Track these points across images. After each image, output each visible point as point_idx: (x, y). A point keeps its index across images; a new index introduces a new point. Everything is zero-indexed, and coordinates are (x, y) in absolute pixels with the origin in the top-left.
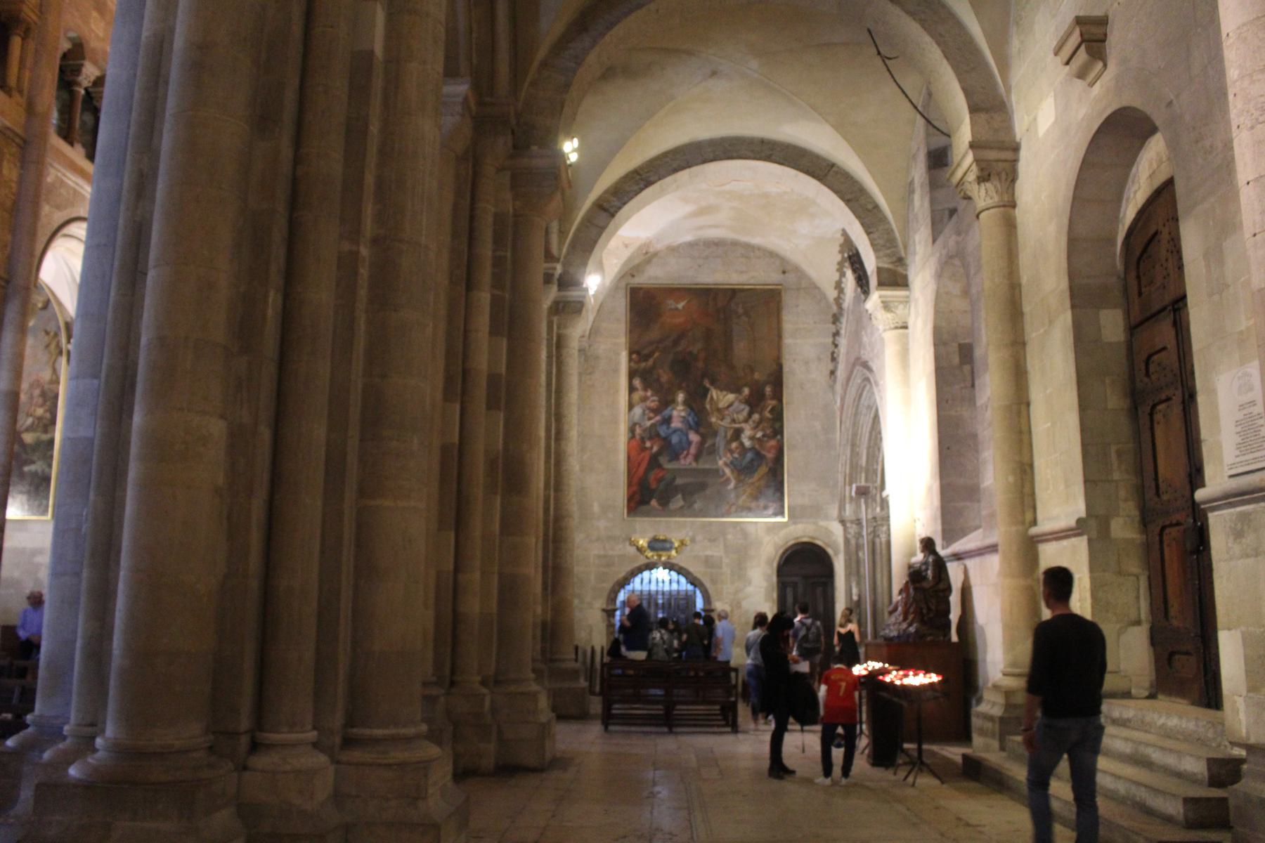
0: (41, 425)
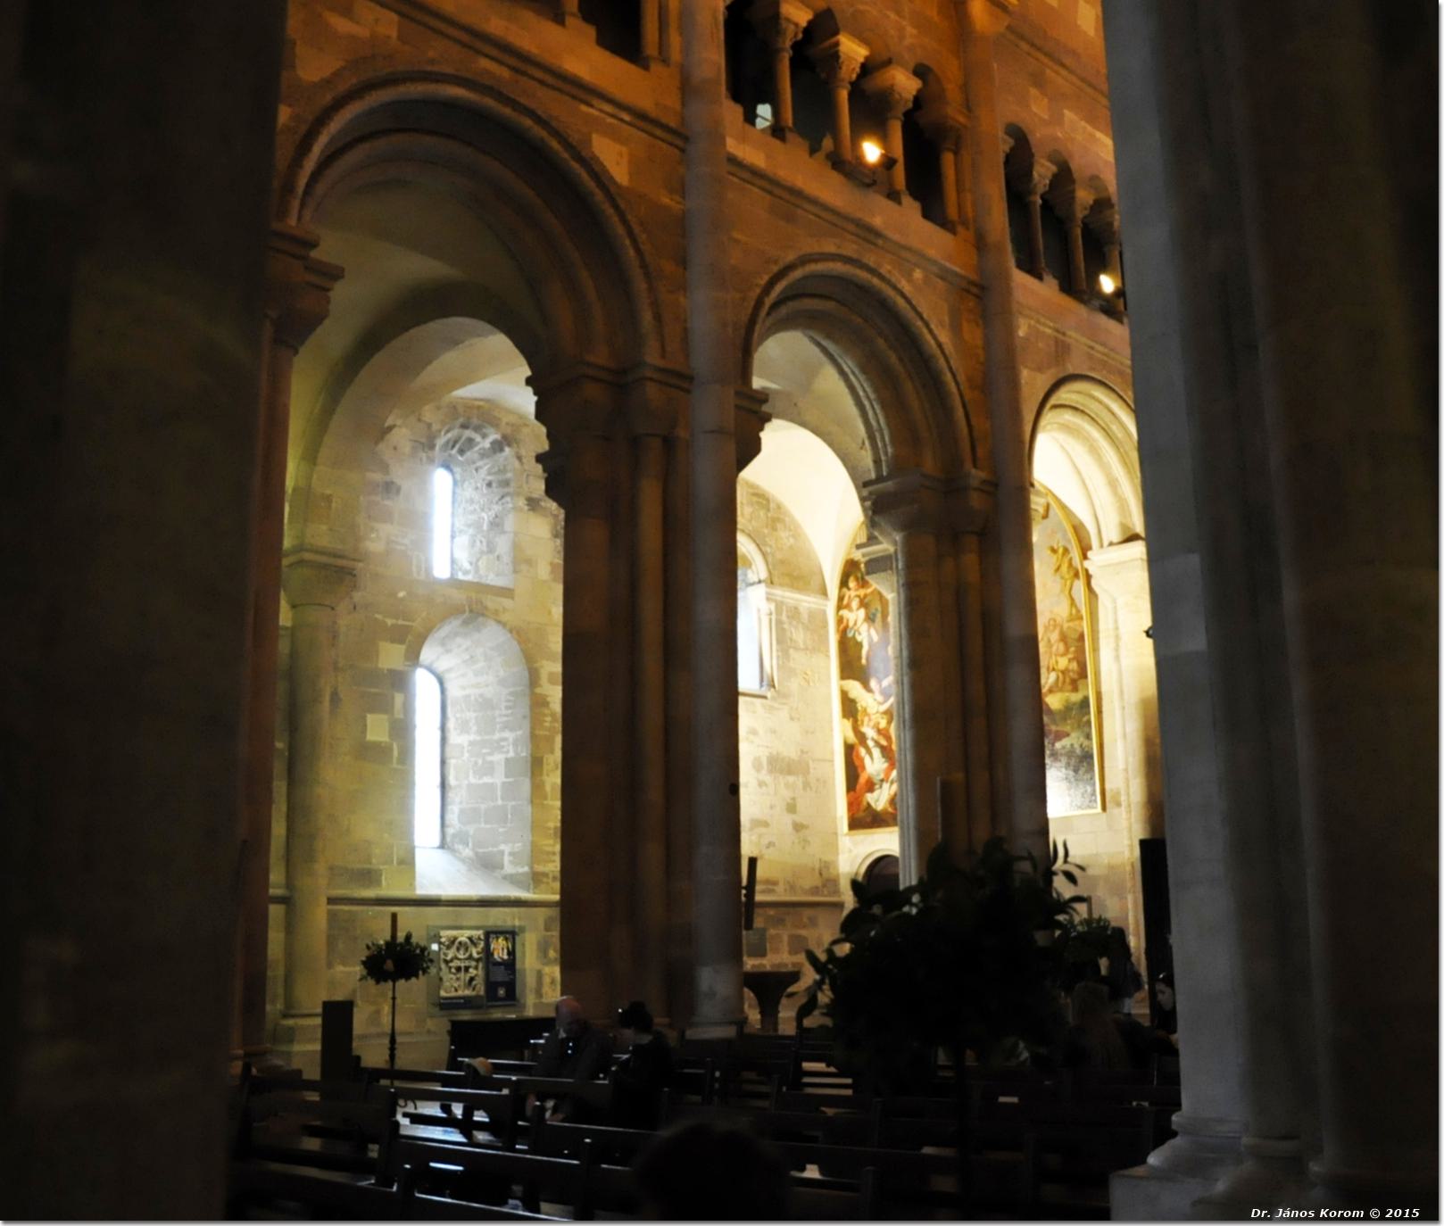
0: (1068, 680)
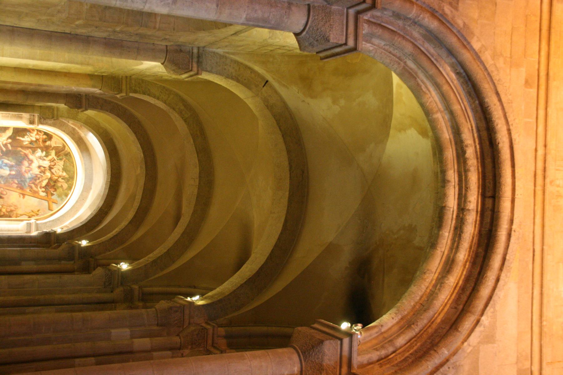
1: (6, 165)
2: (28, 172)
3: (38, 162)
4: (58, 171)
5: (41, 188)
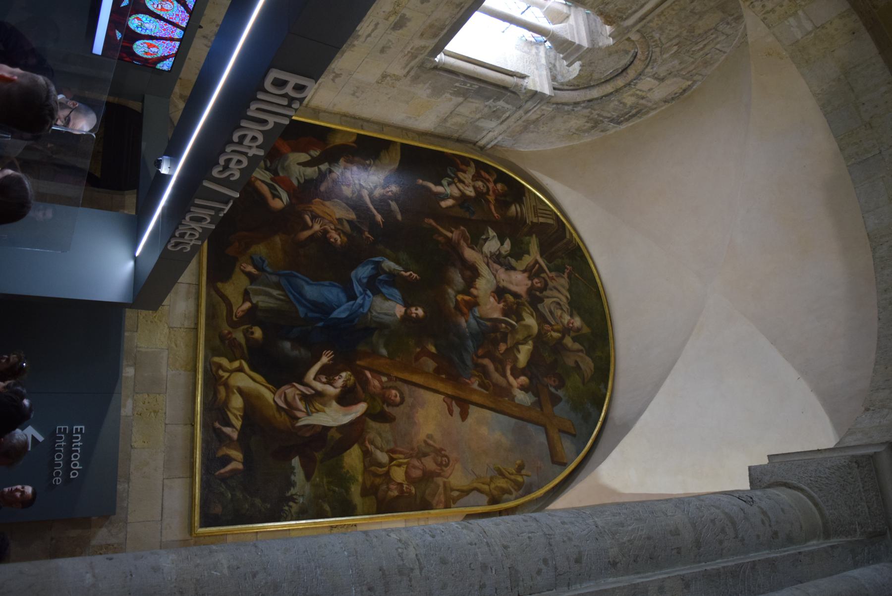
0: (378, 481)
1: (393, 280)
2: (465, 310)
3: (495, 277)
4: (559, 312)
5: (516, 373)
